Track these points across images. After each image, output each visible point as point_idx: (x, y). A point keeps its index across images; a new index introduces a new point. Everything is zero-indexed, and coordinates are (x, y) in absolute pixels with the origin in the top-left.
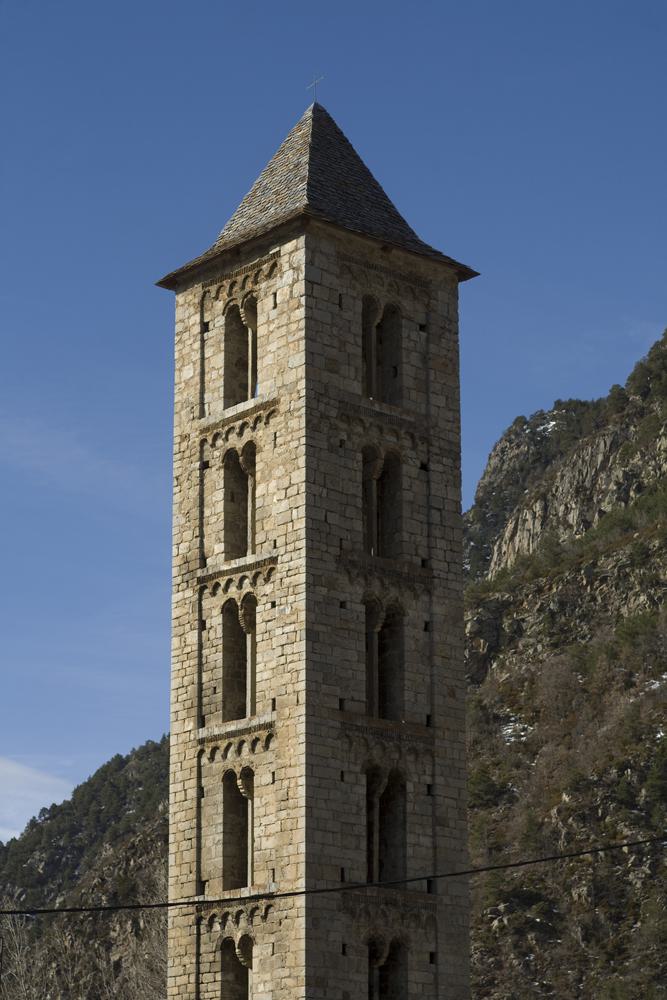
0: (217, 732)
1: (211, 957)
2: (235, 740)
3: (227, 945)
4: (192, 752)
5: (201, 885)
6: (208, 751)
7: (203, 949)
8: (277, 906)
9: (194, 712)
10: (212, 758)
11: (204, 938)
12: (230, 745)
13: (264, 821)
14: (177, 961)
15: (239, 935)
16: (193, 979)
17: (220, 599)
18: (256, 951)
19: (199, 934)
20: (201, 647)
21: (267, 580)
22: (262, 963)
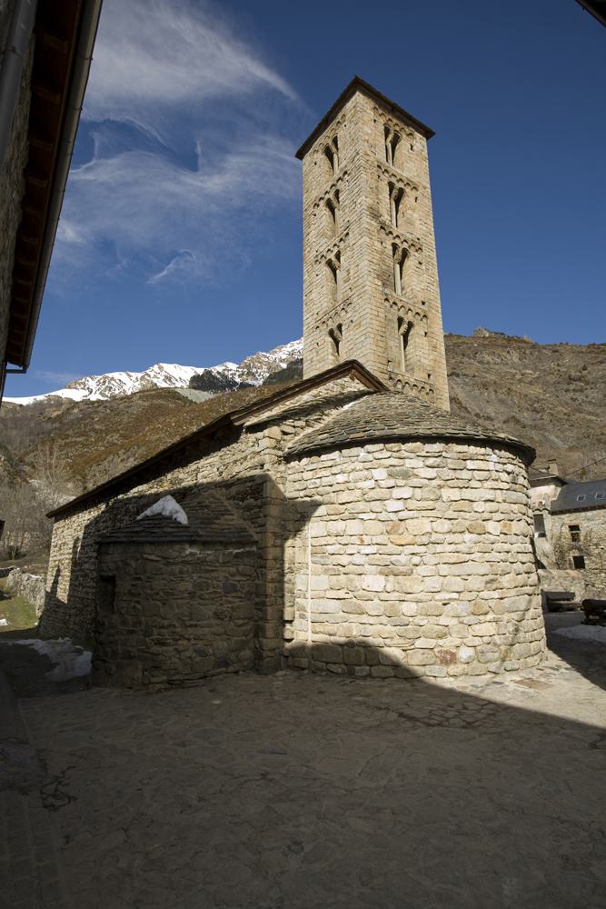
21: (417, 251)
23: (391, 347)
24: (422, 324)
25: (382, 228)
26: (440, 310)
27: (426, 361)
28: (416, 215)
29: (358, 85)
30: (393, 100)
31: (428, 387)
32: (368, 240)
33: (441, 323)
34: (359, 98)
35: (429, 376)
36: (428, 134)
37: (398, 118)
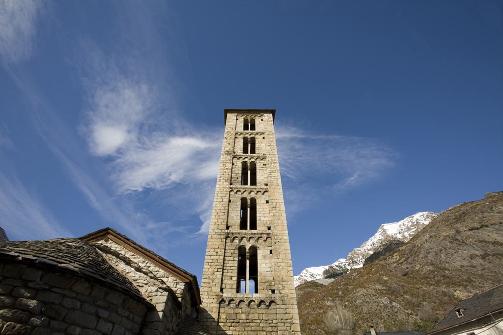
0: (240, 187)
1: (232, 251)
2: (249, 190)
3: (241, 250)
4: (227, 191)
5: (228, 228)
6: (235, 191)
7: (227, 248)
8: (273, 238)
9: (229, 181)
10: (236, 193)
11: (229, 244)
12: (245, 191)
13: (262, 213)
14: (212, 250)
15: (250, 245)
16: (222, 257)
17: (241, 160)
18: (259, 252)
19: (226, 242)
20: (232, 168)
21: (261, 160)
22: (265, 257)
23: (233, 217)
24: (264, 196)
25: (233, 158)
26: (280, 184)
27: (266, 219)
28: (262, 145)
29: (227, 111)
30: (246, 108)
31: (265, 237)
32: (222, 165)
33: (282, 191)
34: (229, 115)
35: (269, 228)
36: (273, 112)
37: (253, 113)
